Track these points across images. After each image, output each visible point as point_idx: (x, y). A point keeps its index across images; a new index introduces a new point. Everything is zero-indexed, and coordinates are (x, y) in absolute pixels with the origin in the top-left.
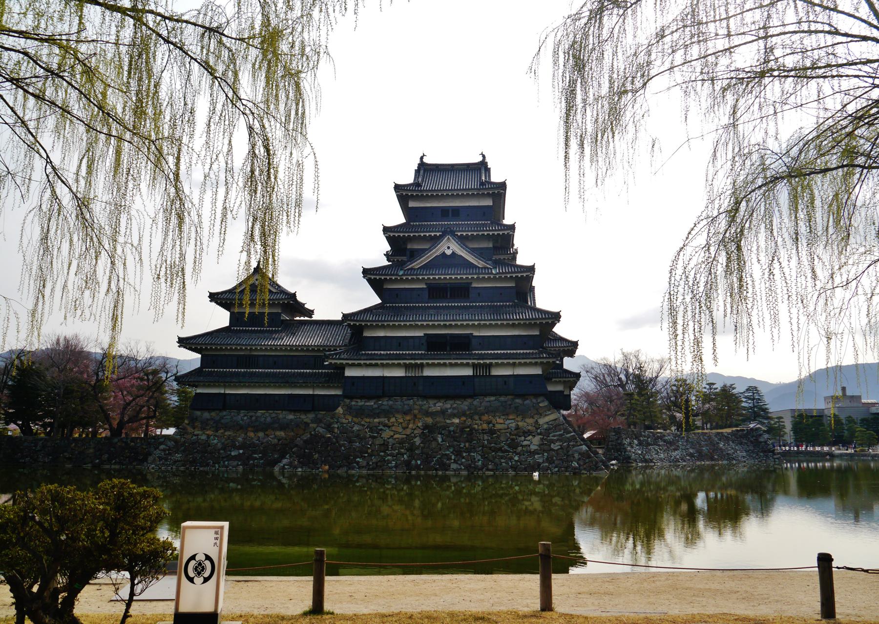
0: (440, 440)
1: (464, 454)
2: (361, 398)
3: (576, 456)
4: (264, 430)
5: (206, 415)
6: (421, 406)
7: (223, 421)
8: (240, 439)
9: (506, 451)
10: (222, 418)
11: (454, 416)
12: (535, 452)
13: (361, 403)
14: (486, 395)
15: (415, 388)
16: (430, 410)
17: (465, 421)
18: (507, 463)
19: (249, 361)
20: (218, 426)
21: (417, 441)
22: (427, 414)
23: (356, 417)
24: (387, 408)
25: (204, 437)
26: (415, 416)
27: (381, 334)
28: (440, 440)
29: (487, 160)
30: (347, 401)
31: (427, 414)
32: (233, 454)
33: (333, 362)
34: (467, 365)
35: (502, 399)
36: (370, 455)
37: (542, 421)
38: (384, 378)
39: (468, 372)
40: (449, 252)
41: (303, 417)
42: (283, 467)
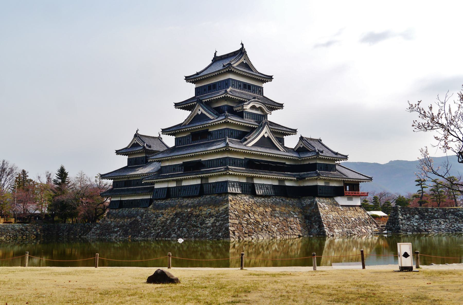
0: (177, 221)
2: (159, 199)
3: (224, 229)
4: (131, 218)
5: (114, 211)
7: (119, 214)
8: (121, 223)
9: (198, 227)
10: (119, 212)
11: (190, 207)
12: (208, 228)
13: (159, 202)
14: (206, 195)
15: (181, 192)
17: (192, 210)
18: (194, 234)
19: (128, 183)
20: (117, 216)
21: (168, 221)
22: (181, 207)
23: (154, 210)
24: (168, 204)
25: (109, 222)
28: (177, 221)
29: (245, 47)
30: (155, 201)
31: (181, 207)
32: (115, 230)
33: (145, 181)
34: (199, 178)
35: (212, 196)
36: (148, 230)
38: (168, 188)
39: (199, 182)
40: (199, 113)
42: (117, 236)
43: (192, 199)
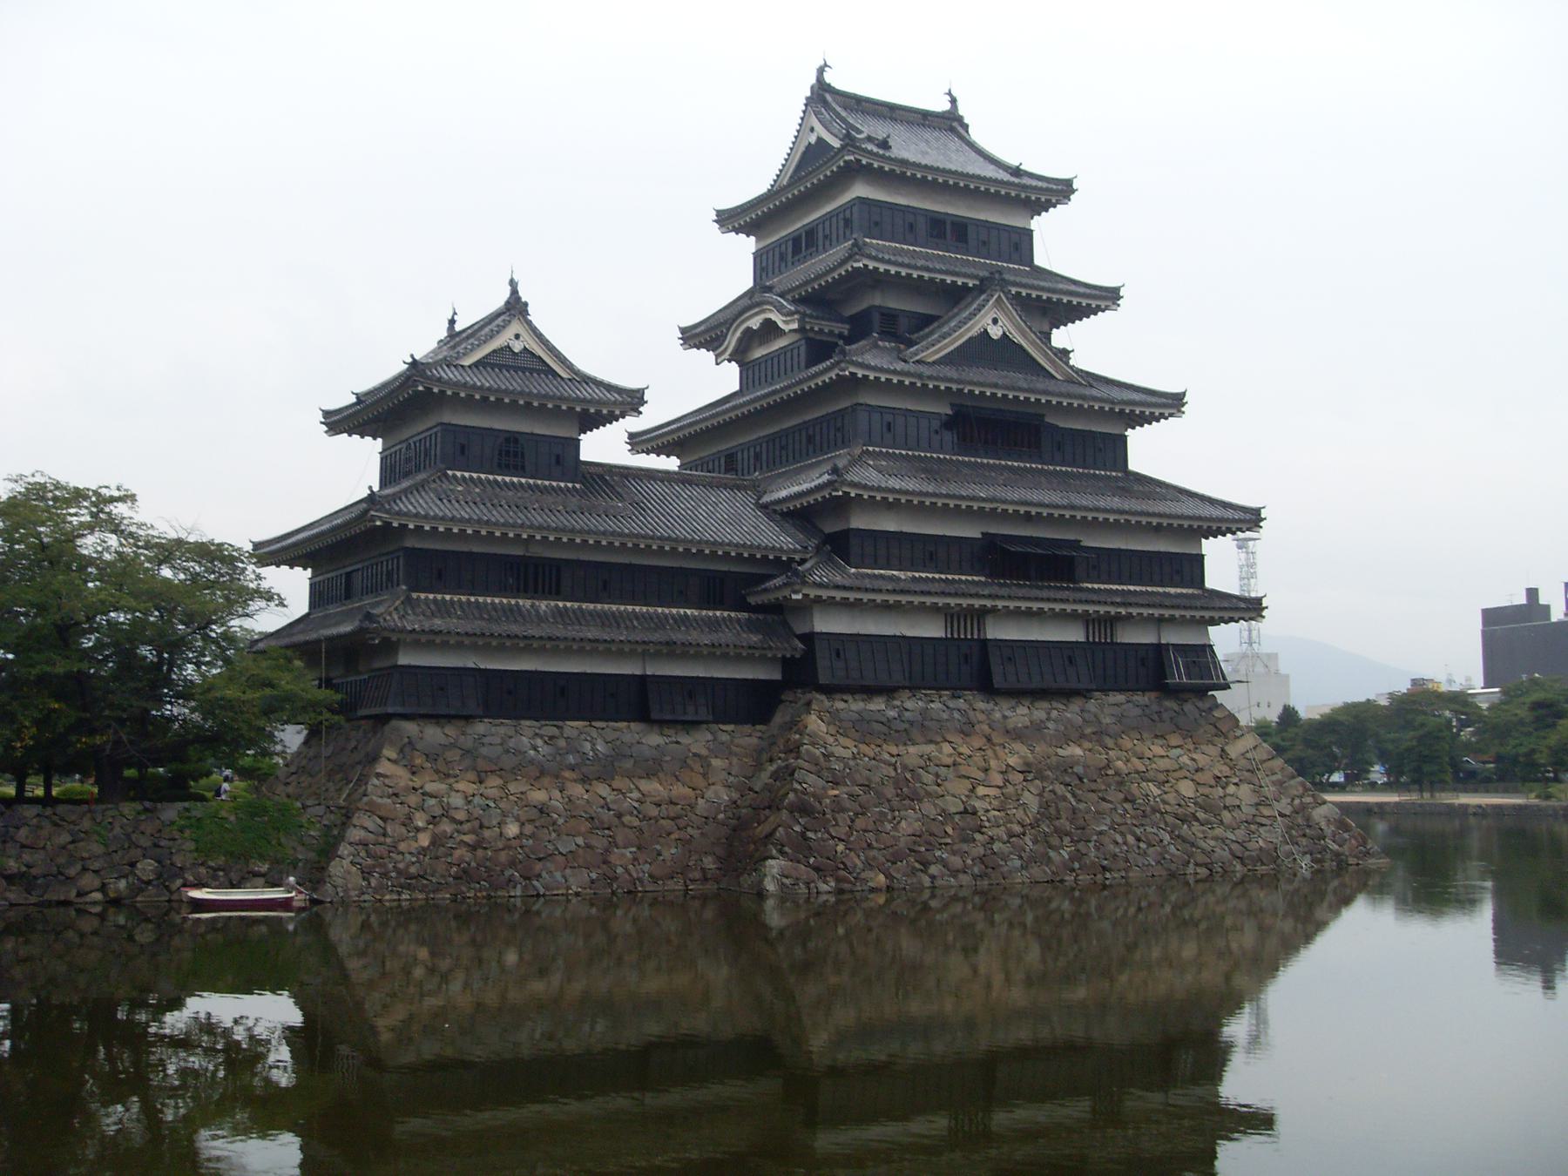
1: (1138, 831)
5: (433, 734)
6: (988, 713)
7: (484, 751)
11: (1067, 740)
13: (856, 705)
14: (1105, 691)
16: (1010, 726)
26: (989, 740)
27: (890, 524)
33: (813, 593)
34: (1074, 616)
35: (1141, 698)
37: (1234, 750)
39: (1074, 634)
40: (995, 332)
41: (685, 739)
43: (1045, 705)
